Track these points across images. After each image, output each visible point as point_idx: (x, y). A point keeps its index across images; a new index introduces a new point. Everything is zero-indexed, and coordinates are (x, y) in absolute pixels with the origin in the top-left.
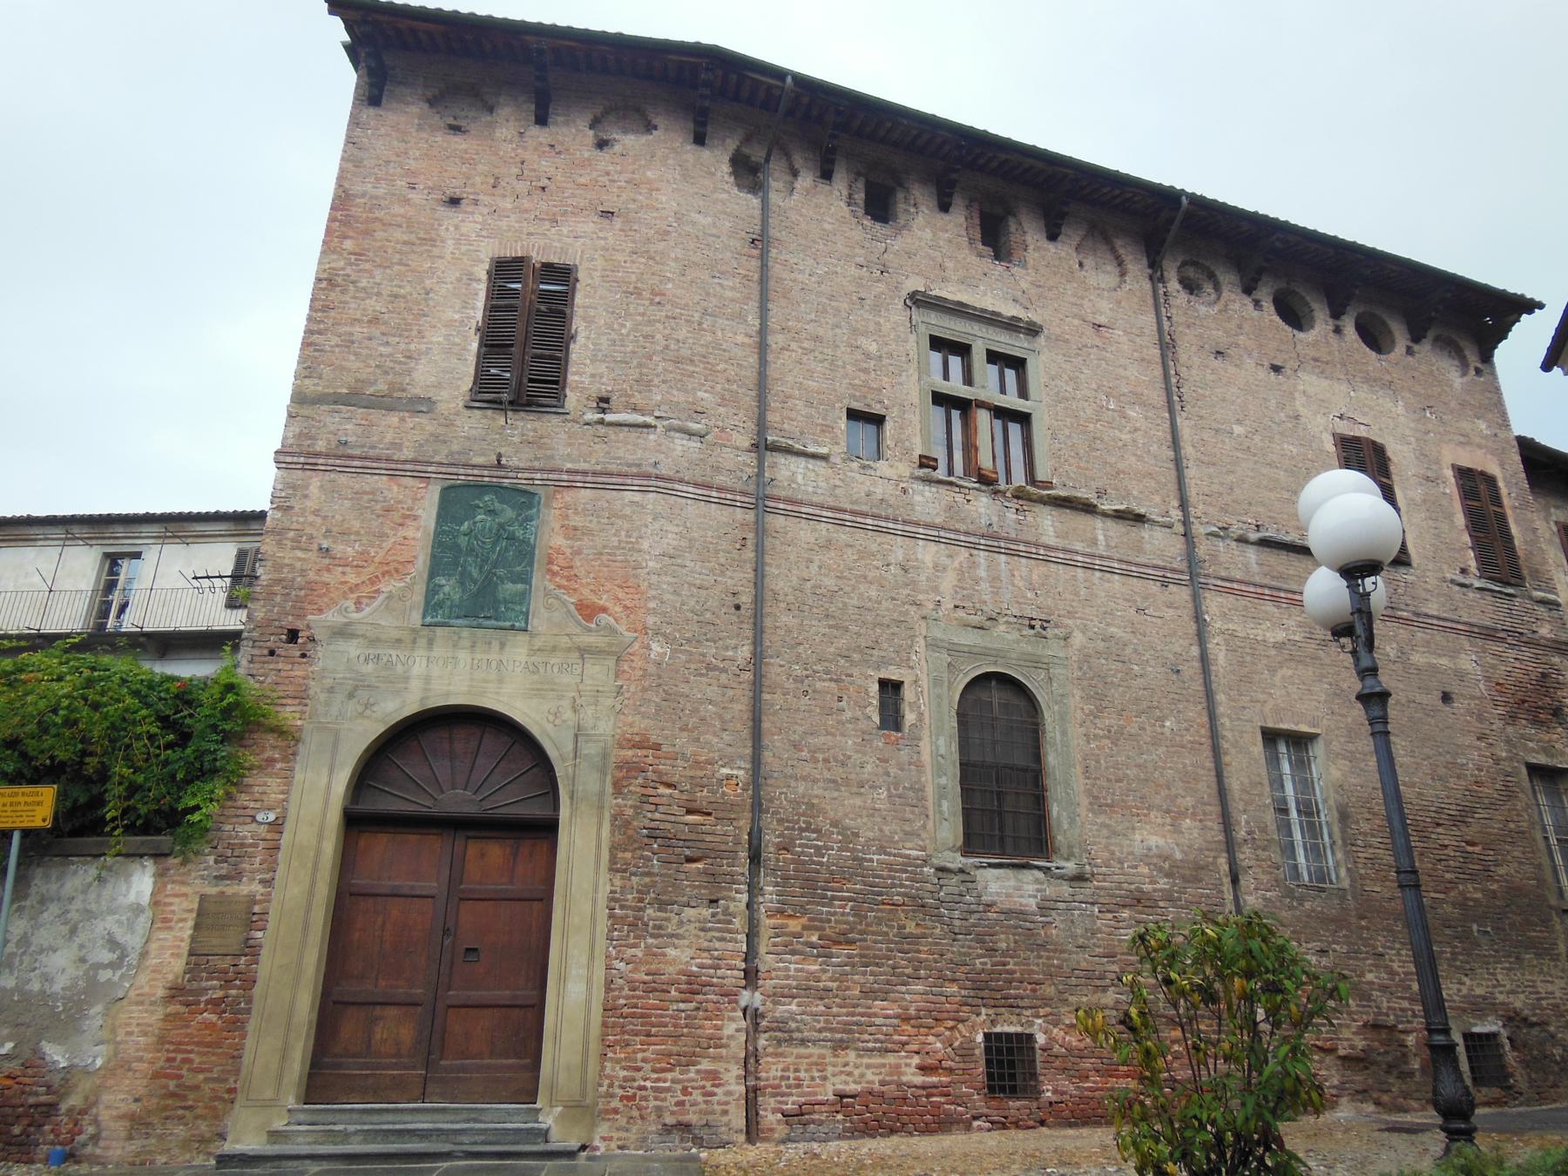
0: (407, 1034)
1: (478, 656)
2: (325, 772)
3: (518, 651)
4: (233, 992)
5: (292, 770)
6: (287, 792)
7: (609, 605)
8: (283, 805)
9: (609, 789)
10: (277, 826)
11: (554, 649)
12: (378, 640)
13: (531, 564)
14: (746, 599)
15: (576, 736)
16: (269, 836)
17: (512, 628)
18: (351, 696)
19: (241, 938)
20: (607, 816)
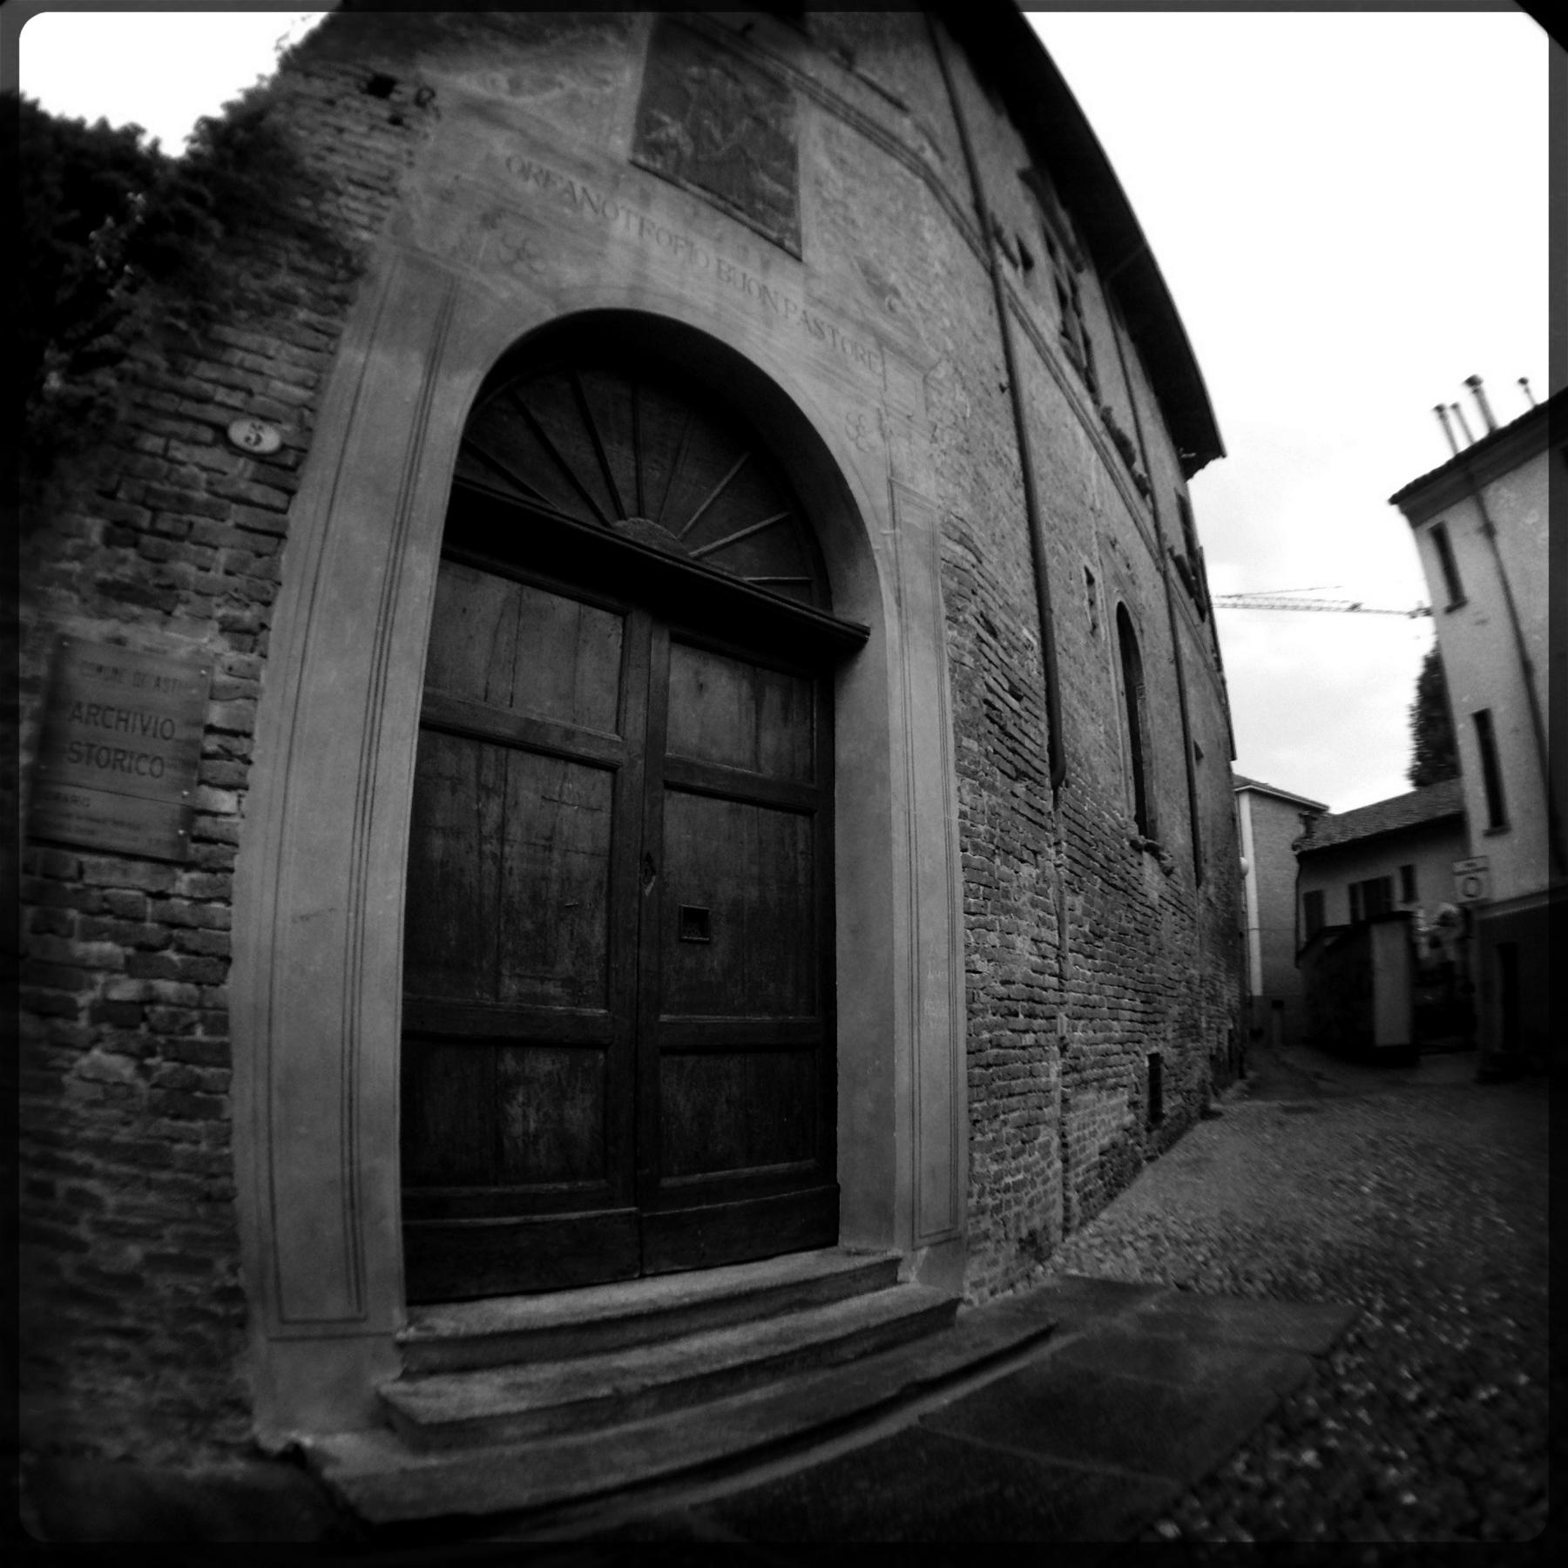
0: (580, 1115)
1: (729, 261)
2: (416, 359)
3: (786, 284)
4: (167, 987)
5: (334, 335)
6: (316, 387)
7: (902, 290)
8: (304, 419)
9: (944, 611)
10: (283, 470)
11: (841, 313)
12: (549, 149)
13: (793, 164)
14: (1004, 380)
15: (890, 482)
16: (257, 493)
17: (779, 244)
18: (489, 220)
19: (175, 802)
20: (947, 665)
